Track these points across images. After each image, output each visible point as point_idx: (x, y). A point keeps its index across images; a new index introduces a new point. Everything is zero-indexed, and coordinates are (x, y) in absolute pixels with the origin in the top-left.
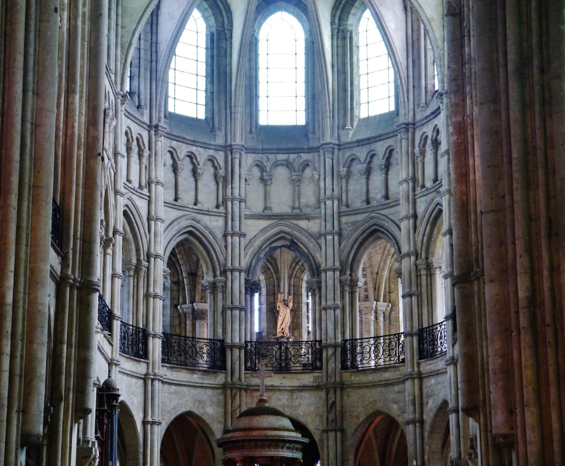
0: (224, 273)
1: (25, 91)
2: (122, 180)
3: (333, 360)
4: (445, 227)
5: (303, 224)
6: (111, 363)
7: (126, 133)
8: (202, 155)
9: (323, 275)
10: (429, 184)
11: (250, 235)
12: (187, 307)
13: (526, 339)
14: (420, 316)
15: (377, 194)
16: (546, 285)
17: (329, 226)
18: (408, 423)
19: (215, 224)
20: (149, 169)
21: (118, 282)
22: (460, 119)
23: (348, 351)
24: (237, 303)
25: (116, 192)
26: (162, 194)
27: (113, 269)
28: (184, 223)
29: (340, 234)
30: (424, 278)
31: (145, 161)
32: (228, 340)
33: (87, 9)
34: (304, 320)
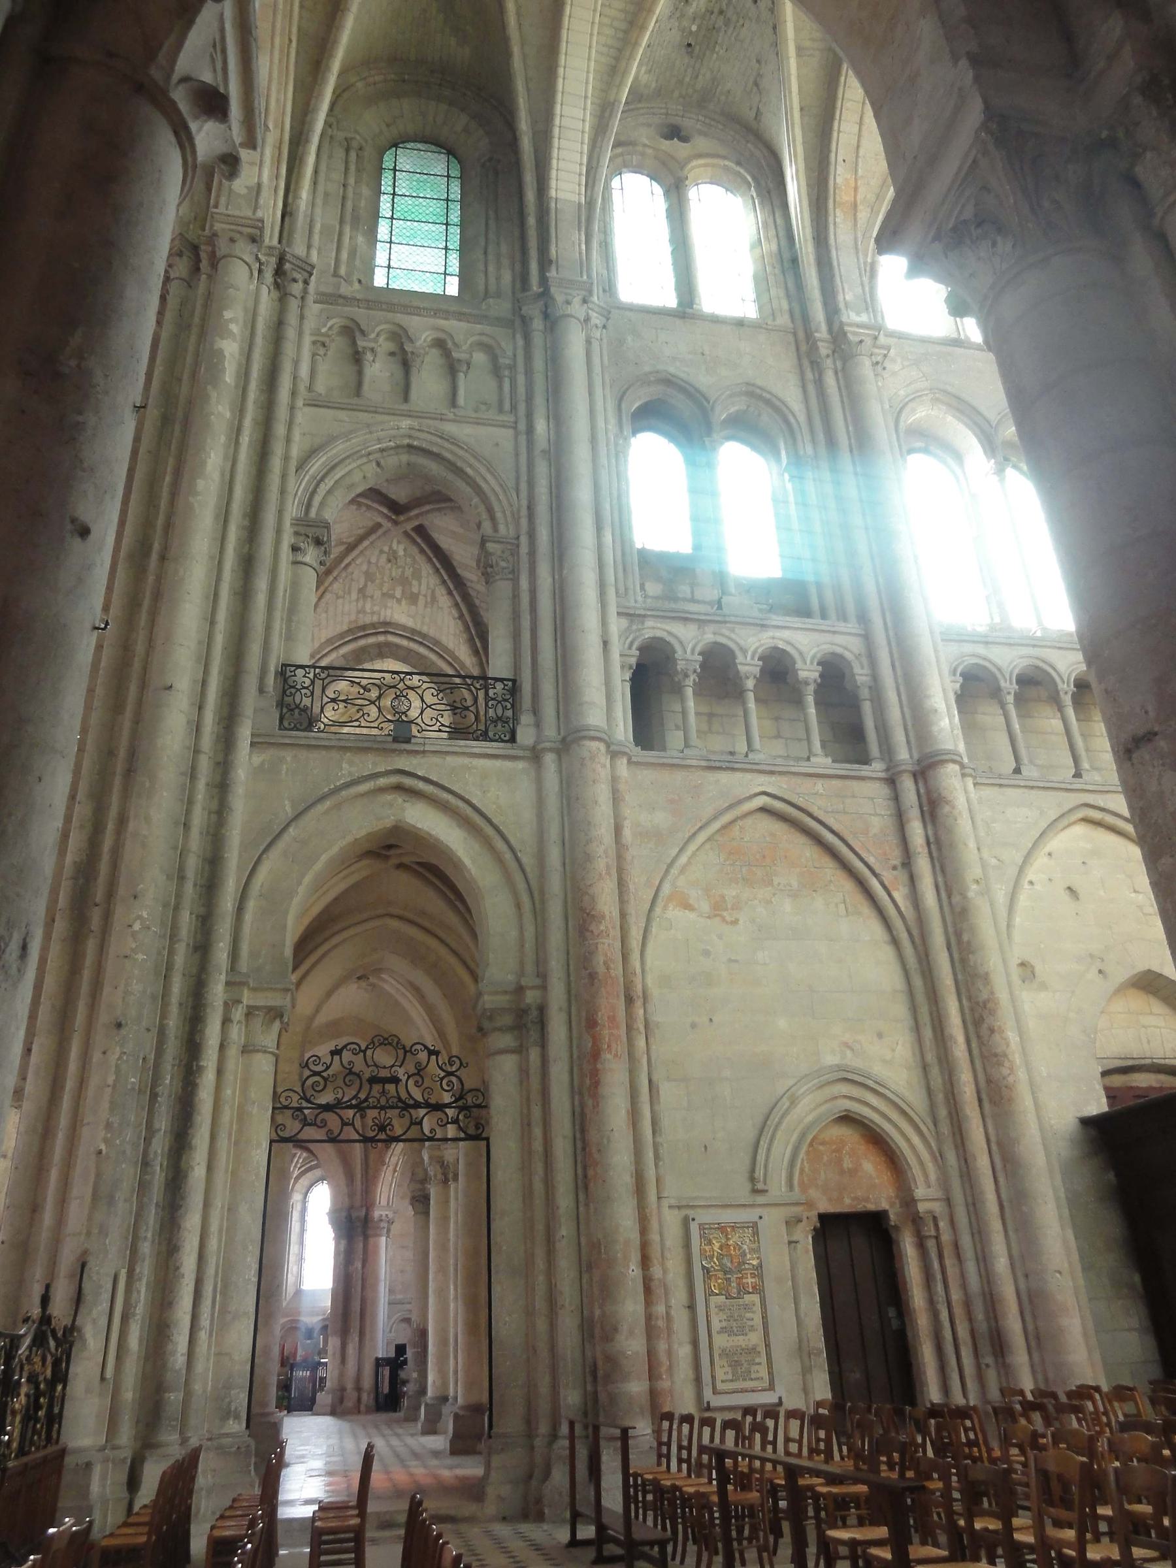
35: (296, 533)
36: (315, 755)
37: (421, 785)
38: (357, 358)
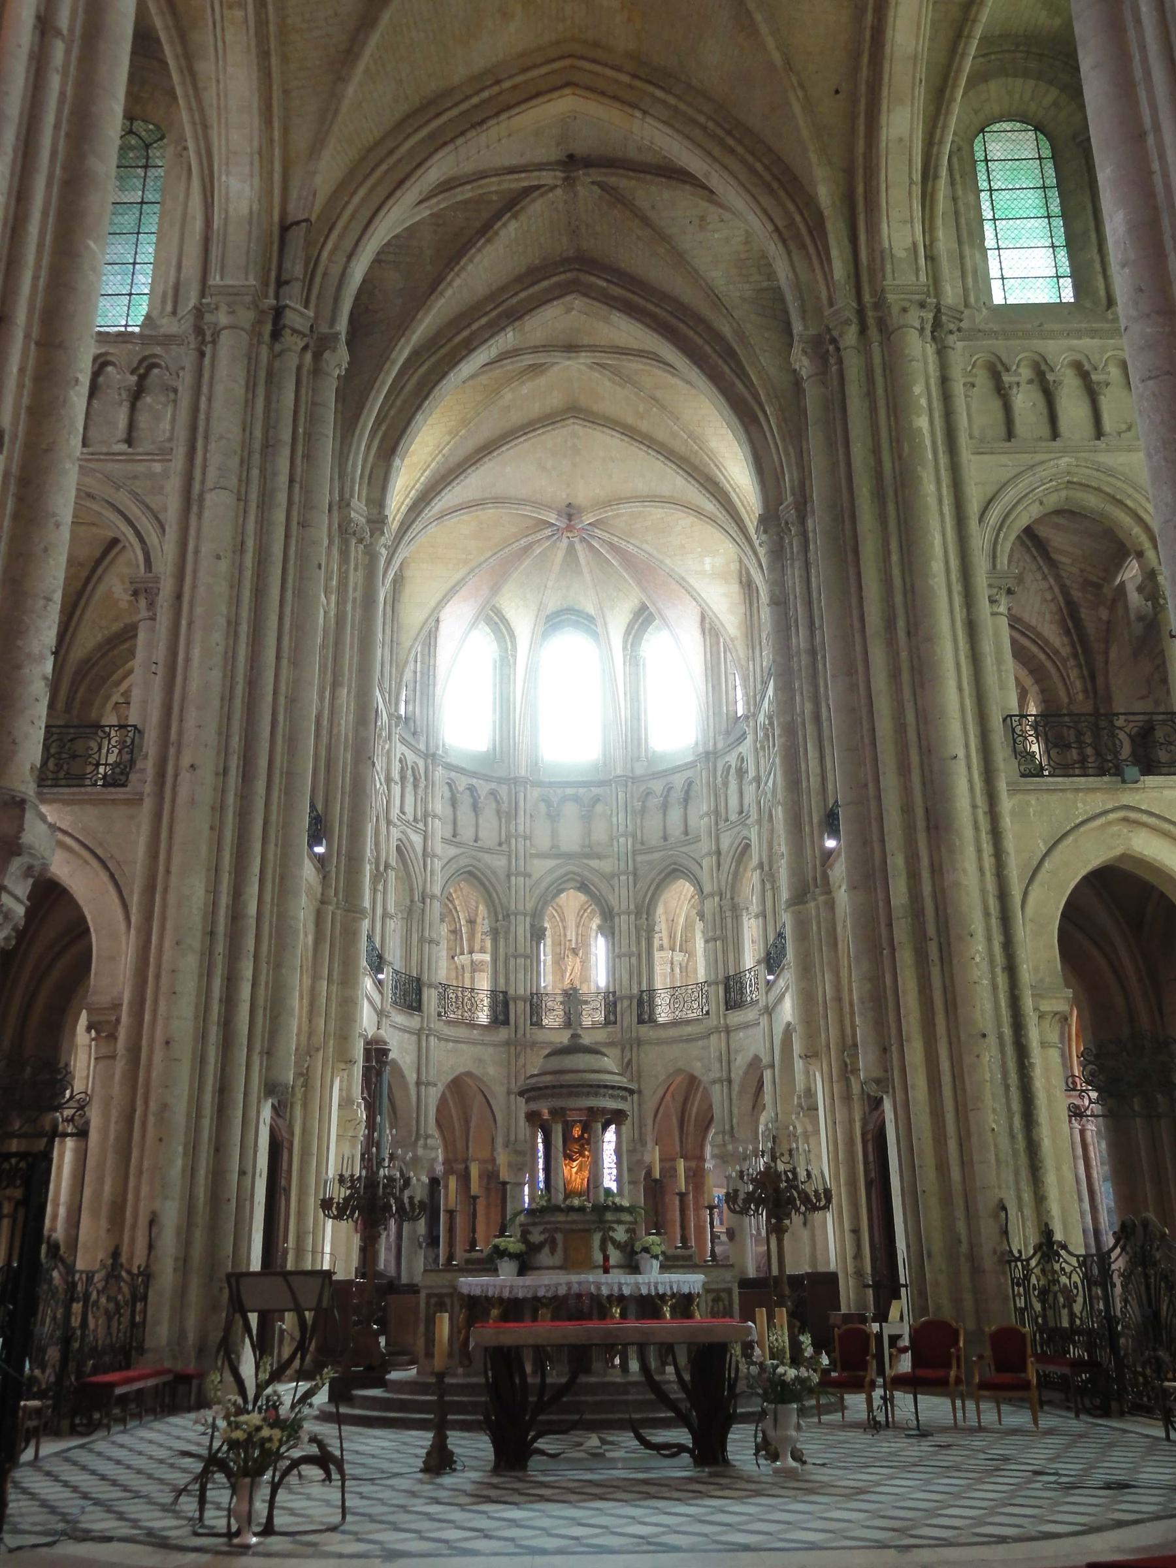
0: (507, 917)
1: (278, 657)
2: (395, 811)
3: (627, 1015)
4: (755, 861)
5: (594, 863)
6: (381, 1013)
7: (401, 761)
8: (483, 788)
9: (617, 919)
10: (733, 817)
11: (536, 877)
12: (464, 959)
13: (906, 957)
14: (725, 963)
16: (927, 889)
17: (622, 864)
18: (714, 1082)
20: (425, 801)
21: (391, 924)
22: (789, 718)
23: (644, 1004)
24: (521, 950)
25: (389, 822)
26: (439, 829)
27: (385, 909)
28: (463, 862)
29: (635, 874)
30: (729, 920)
31: (421, 792)
32: (511, 992)
33: (358, 594)
34: (593, 972)
35: (990, 586)
36: (1055, 797)
37: (1145, 818)
38: (1002, 392)
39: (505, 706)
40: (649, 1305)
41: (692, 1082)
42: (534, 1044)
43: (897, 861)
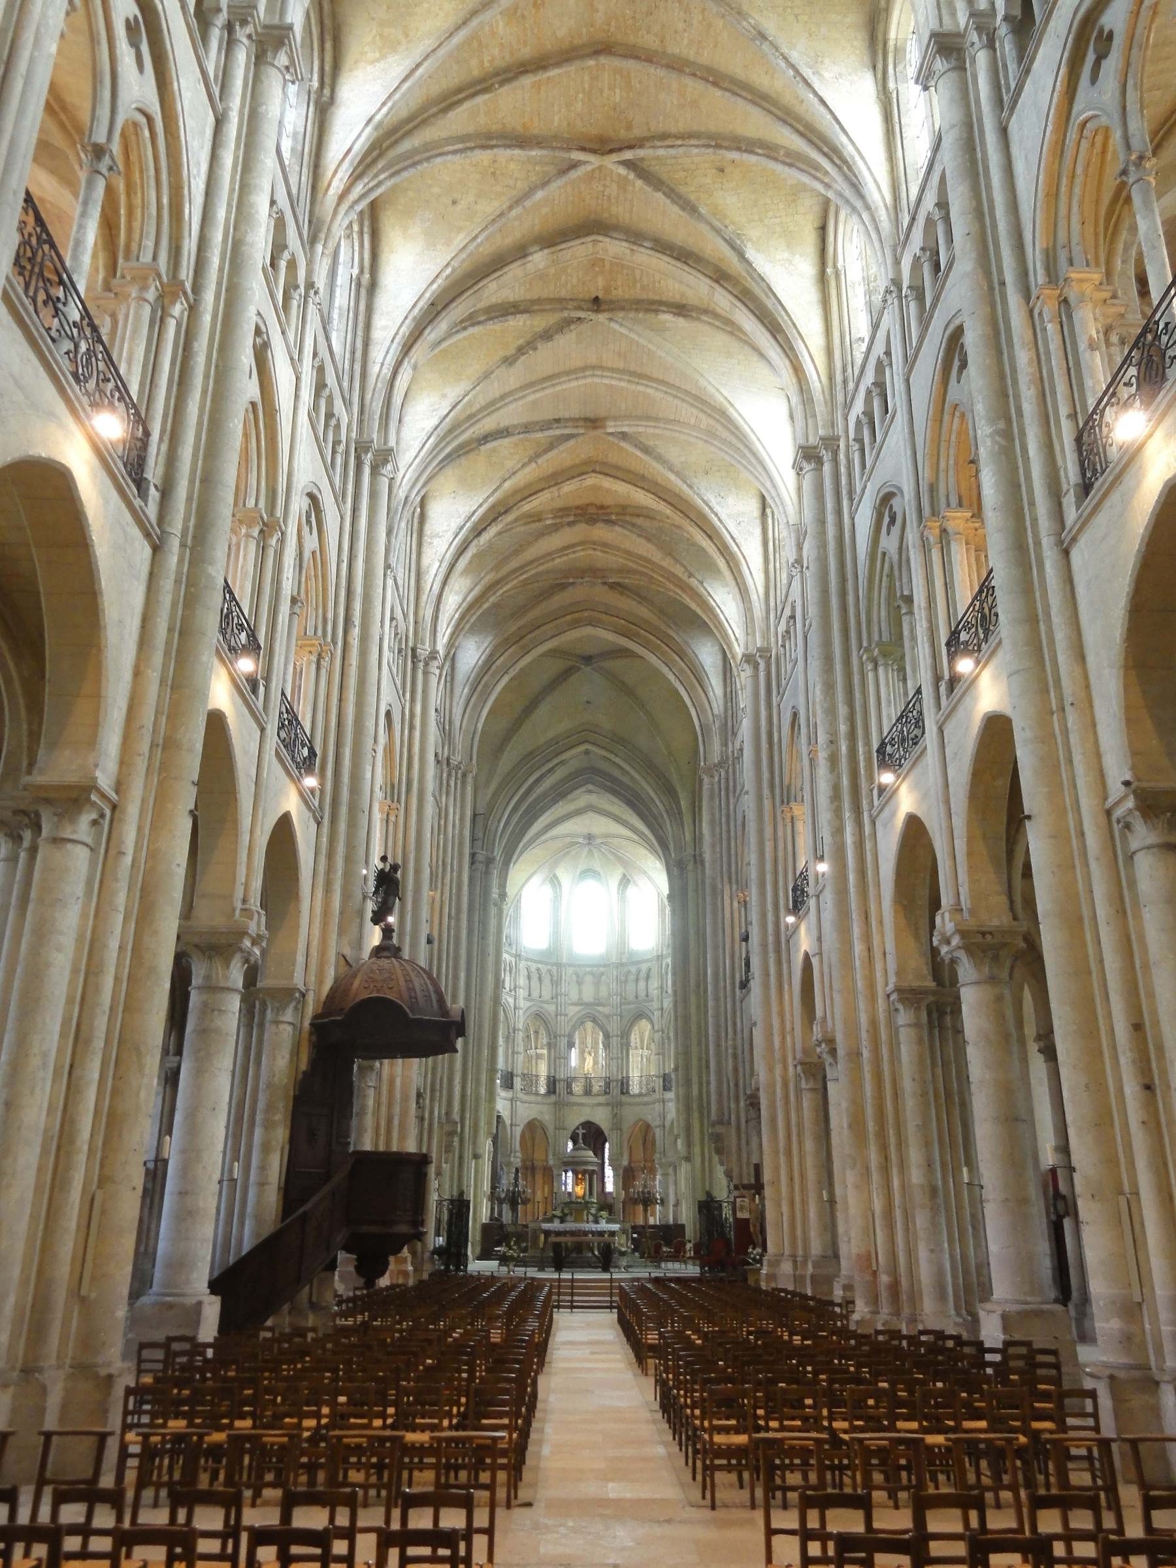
5: (600, 1008)
12: (532, 1052)
13: (696, 1115)
15: (642, 994)
19: (551, 1008)
23: (624, 1084)
26: (522, 993)
39: (556, 924)
40: (601, 1234)
41: (647, 1127)
42: (567, 1104)
43: (695, 1079)
